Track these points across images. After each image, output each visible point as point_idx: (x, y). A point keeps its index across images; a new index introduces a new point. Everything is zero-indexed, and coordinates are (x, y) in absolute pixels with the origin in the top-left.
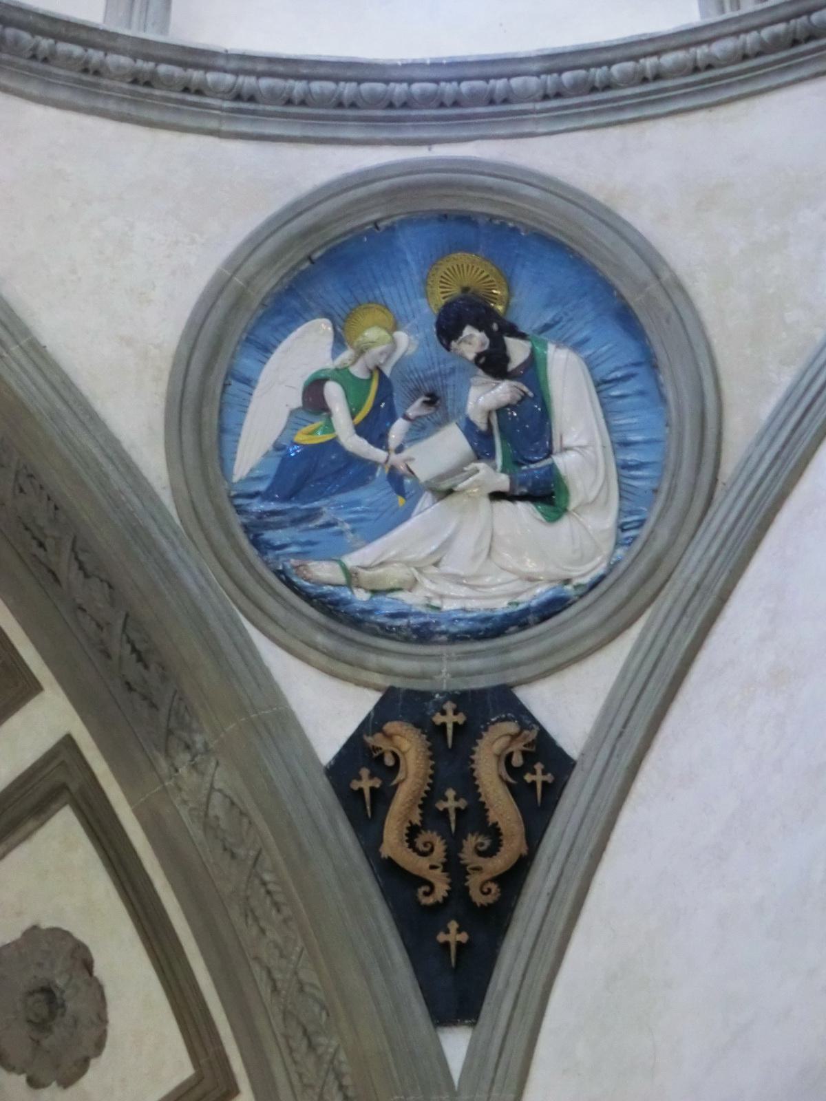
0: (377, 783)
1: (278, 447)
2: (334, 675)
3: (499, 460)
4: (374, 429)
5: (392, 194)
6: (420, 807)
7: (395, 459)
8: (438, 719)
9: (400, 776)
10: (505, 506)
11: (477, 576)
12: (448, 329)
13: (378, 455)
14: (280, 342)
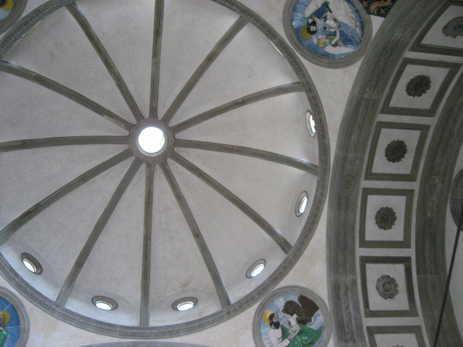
0: (381, 10)
1: (346, 46)
2: (371, 23)
3: (326, 14)
4: (334, 34)
5: (301, 50)
6: (381, 1)
7: (336, 28)
8: (366, 5)
9: (378, 7)
10: (332, 10)
11: (344, 9)
12: (314, 33)
13: (338, 32)
14: (331, 54)
